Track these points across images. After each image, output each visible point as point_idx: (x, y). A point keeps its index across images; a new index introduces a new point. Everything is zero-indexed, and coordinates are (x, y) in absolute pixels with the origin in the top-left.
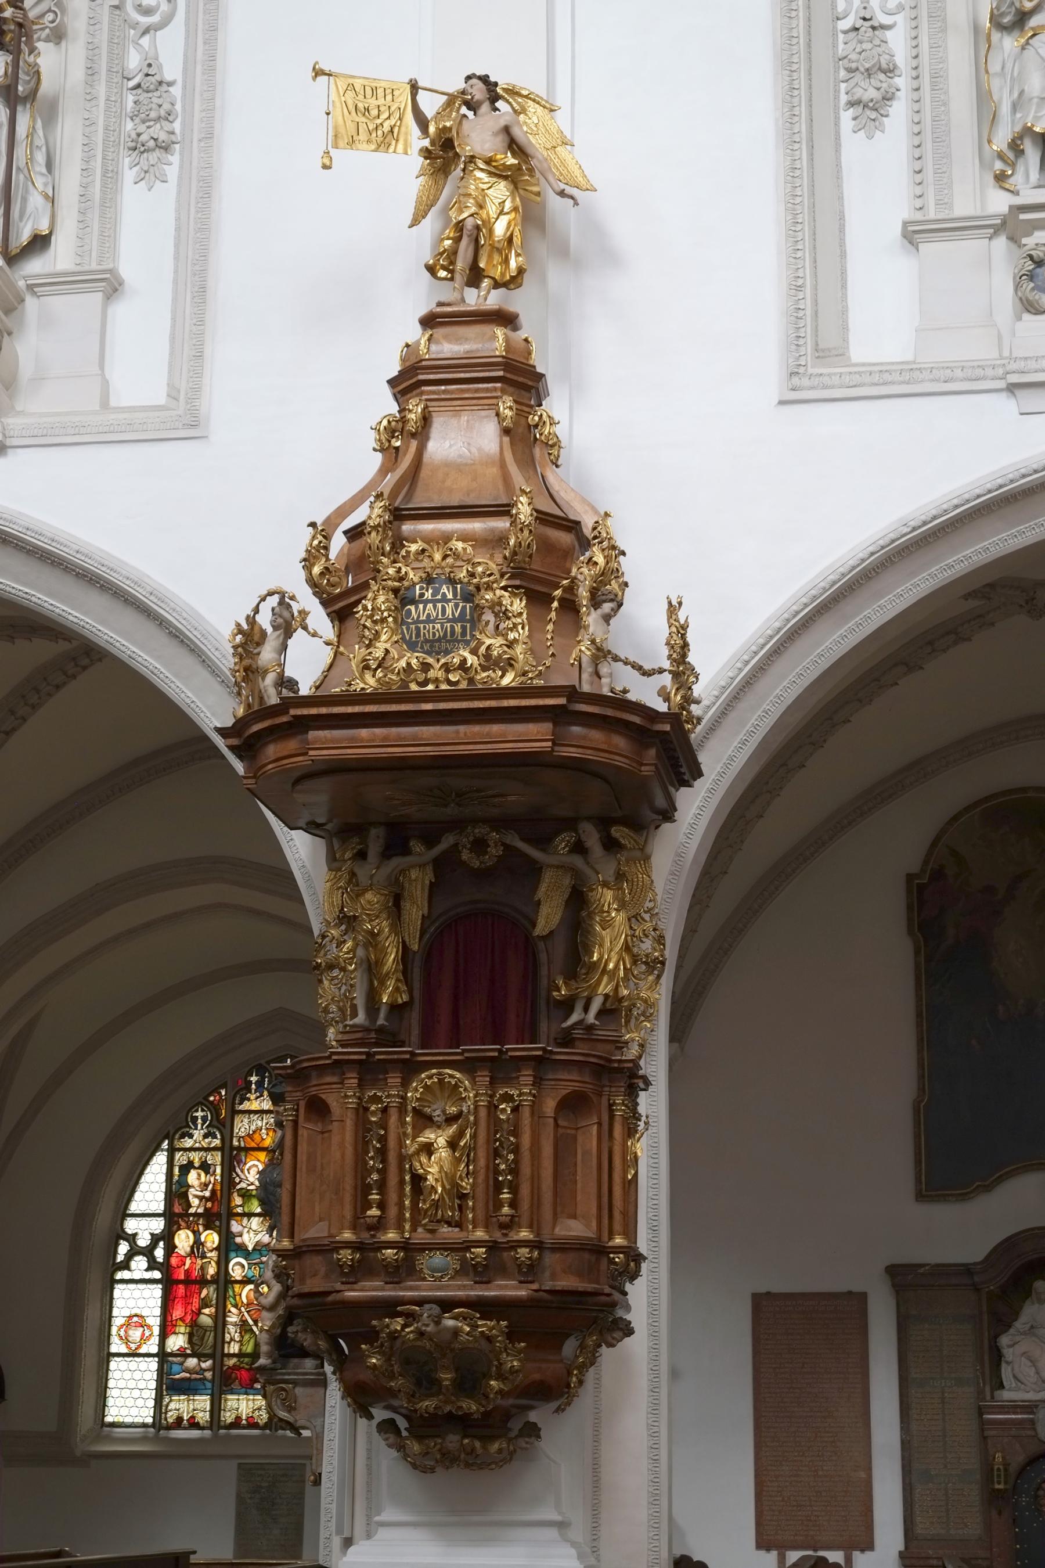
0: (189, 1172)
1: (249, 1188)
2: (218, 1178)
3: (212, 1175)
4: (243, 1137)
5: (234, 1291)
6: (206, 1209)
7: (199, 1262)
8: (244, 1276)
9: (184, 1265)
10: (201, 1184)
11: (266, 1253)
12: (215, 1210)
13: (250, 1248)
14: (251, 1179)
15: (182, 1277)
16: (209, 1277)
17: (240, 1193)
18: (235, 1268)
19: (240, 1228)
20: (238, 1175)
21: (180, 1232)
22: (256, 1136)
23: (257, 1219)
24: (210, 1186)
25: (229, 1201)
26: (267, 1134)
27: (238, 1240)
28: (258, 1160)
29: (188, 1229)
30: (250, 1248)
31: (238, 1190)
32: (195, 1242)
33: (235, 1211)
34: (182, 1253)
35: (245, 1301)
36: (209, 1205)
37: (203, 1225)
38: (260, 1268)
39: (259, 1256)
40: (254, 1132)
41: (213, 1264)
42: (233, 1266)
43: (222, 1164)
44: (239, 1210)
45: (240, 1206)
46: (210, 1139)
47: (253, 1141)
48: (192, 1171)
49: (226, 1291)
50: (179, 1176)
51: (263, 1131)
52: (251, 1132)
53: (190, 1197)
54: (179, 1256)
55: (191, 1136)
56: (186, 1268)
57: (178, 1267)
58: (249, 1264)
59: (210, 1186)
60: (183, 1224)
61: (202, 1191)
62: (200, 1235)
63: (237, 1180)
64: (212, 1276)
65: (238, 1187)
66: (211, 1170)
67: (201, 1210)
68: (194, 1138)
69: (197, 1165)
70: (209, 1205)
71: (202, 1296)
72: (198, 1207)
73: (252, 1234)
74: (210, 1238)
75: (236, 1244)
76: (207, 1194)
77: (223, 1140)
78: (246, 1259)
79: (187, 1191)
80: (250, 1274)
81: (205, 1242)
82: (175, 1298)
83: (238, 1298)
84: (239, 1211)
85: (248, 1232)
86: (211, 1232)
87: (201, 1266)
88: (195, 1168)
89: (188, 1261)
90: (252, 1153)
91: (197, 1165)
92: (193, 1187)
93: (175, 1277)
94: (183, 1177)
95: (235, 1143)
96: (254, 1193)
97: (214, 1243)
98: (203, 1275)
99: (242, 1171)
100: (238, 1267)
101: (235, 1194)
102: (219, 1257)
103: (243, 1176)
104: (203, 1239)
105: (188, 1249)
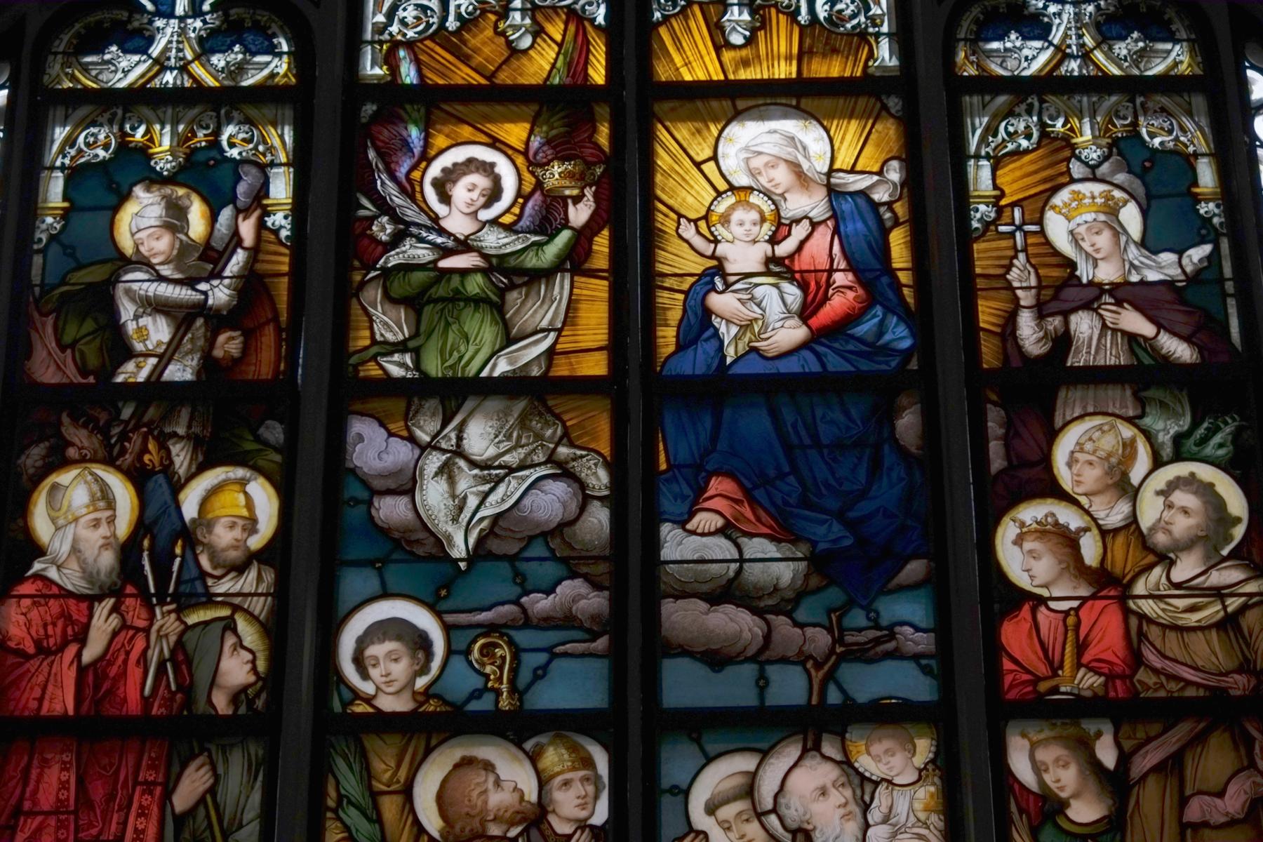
0: (124, 197)
1: (444, 264)
2: (278, 219)
3: (244, 211)
4: (410, 45)
5: (367, 774)
6: (209, 364)
7: (167, 622)
8: (427, 693)
9: (82, 638)
10: (185, 248)
11: (550, 570)
12: (265, 364)
13: (459, 550)
14: (458, 224)
15: (63, 700)
16: (221, 703)
17: (397, 289)
18: (377, 650)
19: (401, 452)
20: (385, 207)
21: (65, 477)
22: (484, 43)
23: (494, 404)
24: (239, 259)
25: (342, 327)
26: (538, 32)
27: (391, 510)
28: (495, 143)
29: (110, 461)
30: (459, 550)
31: (387, 273)
32: (141, 527)
33: (372, 371)
34: (71, 579)
35: (432, 822)
36: (229, 344)
37: (196, 442)
38: (517, 652)
39: (513, 591)
40: (467, 23)
41: (248, 632)
42: (362, 642)
43: (301, 162)
44: (397, 366)
45: (401, 347)
46: (236, 55)
47: (465, 59)
48: (138, 191)
49: (320, 771)
50: (66, 215)
51: (516, 17)
52: (452, 24)
53: (127, 310)
54: (51, 591)
55: (138, 41)
56: (88, 655)
57: (43, 650)
58: (448, 629)
59: (239, 259)
60: (80, 437)
61: (190, 282)
62: (177, 487)
63: (383, 229)
64: (237, 696)
65: (394, 259)
66: (241, 189)
67: (180, 372)
68: (155, 51)
69: (164, 162)
70: (229, 344)
71: (183, 798)
72: (166, 357)
73: (466, 481)
74: (231, 502)
75: (384, 532)
76: (220, 294)
77: (301, 59)
78: (433, 607)
79: (113, 280)
80: (462, 681)
81: (205, 520)
82: (18, 812)
83: (390, 807)
84: (396, 371)
85: (446, 470)
86: (240, 472)
87: (180, 644)
88: (155, 180)
89: (102, 624)
90: (460, 109)
91: (164, 162)
92: (143, 263)
93: (27, 701)
94: (86, 224)
95: (372, 70)
96: (475, 285)
97: (251, 524)
98: (187, 689)
99: (411, 191)
100: (390, 646)
101: (374, 294)
102: (281, 594)
103: (411, 214)
104: (190, 510)
105: (107, 560)
